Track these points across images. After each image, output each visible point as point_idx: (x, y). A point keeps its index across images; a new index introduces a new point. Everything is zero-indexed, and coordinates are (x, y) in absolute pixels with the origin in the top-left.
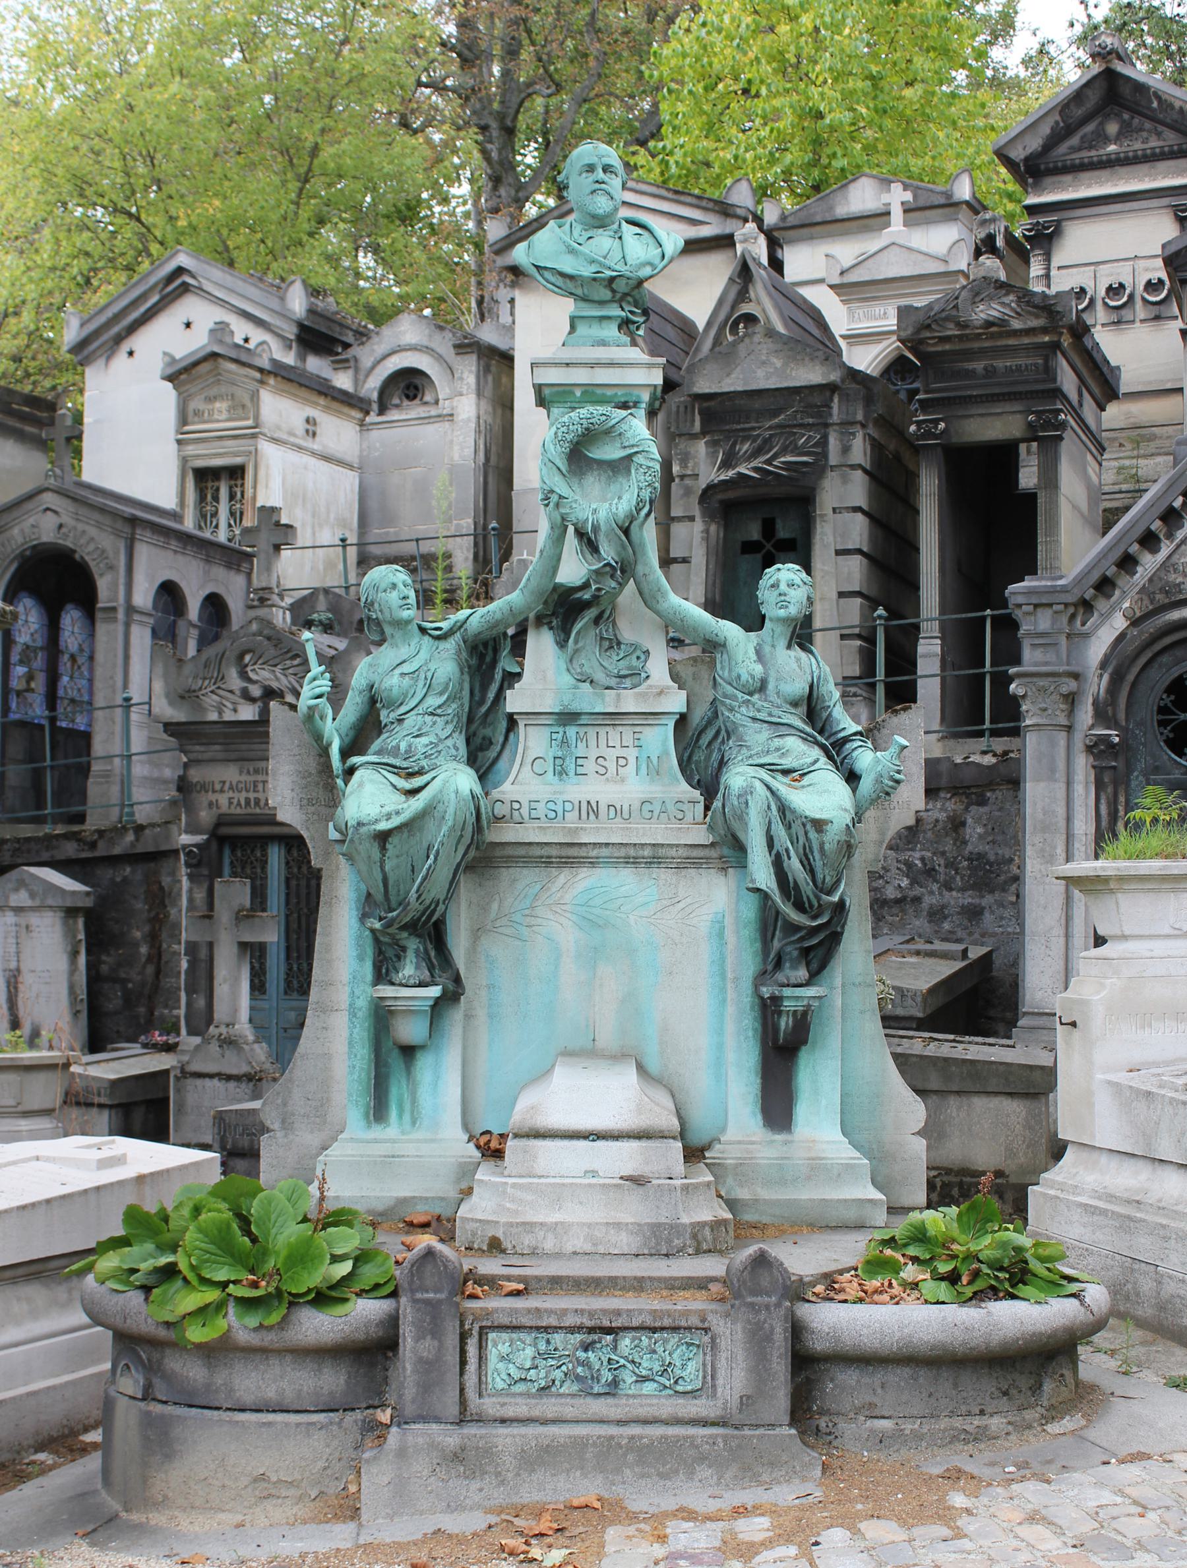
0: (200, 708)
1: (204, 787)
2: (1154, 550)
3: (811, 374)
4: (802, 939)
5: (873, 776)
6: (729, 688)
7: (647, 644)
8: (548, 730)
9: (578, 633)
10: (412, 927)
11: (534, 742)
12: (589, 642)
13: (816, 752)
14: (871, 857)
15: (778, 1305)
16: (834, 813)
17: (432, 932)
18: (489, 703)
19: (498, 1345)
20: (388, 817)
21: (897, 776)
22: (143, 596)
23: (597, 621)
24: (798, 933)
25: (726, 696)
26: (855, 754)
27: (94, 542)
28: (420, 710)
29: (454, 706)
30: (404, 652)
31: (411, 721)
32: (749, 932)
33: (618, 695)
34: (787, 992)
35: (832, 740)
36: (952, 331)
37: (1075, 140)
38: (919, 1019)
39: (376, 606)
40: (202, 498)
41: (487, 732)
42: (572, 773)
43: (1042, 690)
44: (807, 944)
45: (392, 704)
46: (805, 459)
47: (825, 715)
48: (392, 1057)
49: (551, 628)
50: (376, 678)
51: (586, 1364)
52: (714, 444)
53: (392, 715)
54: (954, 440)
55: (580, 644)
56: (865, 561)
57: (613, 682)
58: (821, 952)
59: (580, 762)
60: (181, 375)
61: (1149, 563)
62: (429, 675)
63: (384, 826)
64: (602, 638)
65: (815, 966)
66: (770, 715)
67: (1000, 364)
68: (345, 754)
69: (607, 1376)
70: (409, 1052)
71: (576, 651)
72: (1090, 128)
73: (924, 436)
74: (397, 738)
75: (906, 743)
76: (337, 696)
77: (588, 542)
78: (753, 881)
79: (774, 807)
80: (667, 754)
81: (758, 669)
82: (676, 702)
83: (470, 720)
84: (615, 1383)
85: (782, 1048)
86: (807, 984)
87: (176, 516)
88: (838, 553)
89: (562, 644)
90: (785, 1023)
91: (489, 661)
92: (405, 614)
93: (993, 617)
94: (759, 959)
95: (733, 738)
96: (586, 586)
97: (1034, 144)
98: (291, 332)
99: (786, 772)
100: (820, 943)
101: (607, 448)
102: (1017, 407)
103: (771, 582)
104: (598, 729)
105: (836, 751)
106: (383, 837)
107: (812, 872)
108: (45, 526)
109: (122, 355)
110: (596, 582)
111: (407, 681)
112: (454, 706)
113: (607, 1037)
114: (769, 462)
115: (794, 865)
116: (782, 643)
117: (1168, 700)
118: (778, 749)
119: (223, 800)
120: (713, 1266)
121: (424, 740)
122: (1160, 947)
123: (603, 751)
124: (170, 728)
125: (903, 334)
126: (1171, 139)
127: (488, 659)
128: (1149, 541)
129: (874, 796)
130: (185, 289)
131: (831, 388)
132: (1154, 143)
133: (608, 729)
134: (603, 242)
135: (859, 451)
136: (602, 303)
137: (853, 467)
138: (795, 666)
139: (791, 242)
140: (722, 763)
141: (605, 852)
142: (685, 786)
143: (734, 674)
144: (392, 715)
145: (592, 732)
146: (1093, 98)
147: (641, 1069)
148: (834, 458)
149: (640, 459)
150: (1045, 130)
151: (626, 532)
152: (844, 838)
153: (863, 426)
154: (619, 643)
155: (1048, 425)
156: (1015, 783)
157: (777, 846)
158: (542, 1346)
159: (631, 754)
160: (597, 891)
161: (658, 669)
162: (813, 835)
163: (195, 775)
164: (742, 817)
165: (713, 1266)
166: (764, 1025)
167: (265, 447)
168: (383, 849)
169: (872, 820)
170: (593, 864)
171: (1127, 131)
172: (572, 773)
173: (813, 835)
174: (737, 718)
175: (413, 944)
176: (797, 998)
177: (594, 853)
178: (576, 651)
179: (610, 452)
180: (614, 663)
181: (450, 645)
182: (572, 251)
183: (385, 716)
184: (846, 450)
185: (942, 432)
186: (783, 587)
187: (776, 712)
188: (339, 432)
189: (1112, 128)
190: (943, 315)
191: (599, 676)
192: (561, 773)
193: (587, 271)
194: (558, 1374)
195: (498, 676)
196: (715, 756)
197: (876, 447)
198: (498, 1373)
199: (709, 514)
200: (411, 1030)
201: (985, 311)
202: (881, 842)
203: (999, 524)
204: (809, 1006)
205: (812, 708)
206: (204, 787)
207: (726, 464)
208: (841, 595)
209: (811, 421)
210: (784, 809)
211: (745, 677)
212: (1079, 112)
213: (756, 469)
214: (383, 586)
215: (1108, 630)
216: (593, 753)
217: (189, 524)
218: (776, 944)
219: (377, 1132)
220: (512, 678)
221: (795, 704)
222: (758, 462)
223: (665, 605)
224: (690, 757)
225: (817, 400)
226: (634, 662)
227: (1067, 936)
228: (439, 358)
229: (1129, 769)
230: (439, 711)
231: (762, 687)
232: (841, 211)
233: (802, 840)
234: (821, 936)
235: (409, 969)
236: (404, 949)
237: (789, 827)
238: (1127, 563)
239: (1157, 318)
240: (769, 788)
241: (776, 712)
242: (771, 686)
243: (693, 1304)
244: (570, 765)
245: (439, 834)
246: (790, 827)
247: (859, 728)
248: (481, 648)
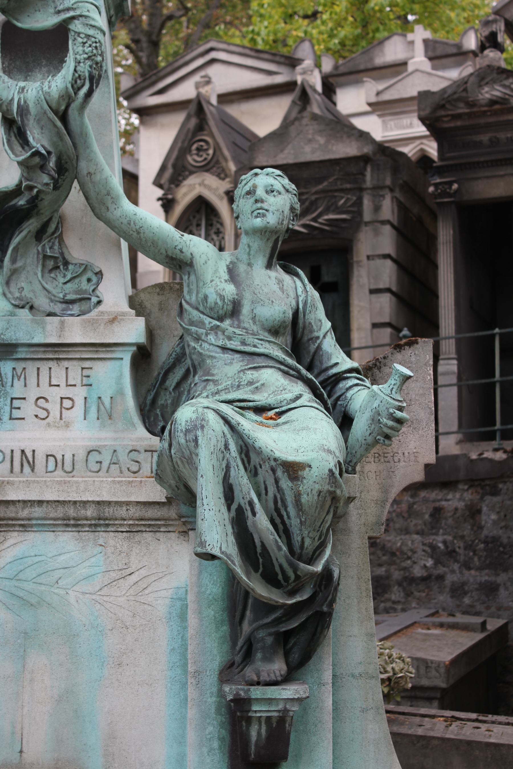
3: (348, 149)
4: (277, 621)
5: (367, 415)
6: (195, 313)
7: (100, 264)
9: (16, 249)
12: (31, 260)
13: (299, 388)
14: (372, 519)
16: (314, 455)
21: (399, 414)
23: (39, 235)
25: (192, 323)
26: (349, 394)
32: (214, 612)
33: (62, 323)
34: (256, 692)
35: (322, 378)
36: (462, 109)
38: (443, 690)
42: (6, 417)
44: (284, 628)
46: (344, 216)
47: (313, 348)
55: (19, 264)
56: (394, 299)
57: (58, 308)
59: (16, 403)
64: (46, 257)
65: (295, 656)
66: (243, 343)
67: (502, 136)
71: (14, 272)
73: (440, 196)
75: (409, 373)
78: (202, 544)
79: (233, 447)
80: (121, 392)
81: (230, 290)
82: (133, 331)
86: (287, 679)
88: (372, 292)
90: (255, 733)
93: (501, 335)
94: (226, 647)
95: (200, 373)
99: (260, 410)
100: (302, 627)
101: (39, 15)
103: (247, 188)
104: (38, 364)
105: (327, 390)
110: (27, 179)
114: (315, 220)
116: (260, 262)
118: (250, 383)
123: (45, 390)
125: (423, 114)
129: (370, 439)
131: (364, 160)
133: (51, 364)
135: (388, 209)
137: (383, 222)
138: (276, 288)
139: (342, 85)
141: (38, 512)
143: (201, 296)
145: (31, 368)
151: (64, 117)
152: (327, 487)
153: (391, 190)
154: (66, 263)
157: (239, 499)
159: (79, 394)
160: (29, 561)
161: (114, 293)
162: (285, 484)
164: (191, 460)
169: (372, 475)
170: (25, 528)
172: (6, 417)
173: (285, 484)
174: (204, 348)
176: (270, 701)
177: (25, 513)
178: (14, 272)
180: (59, 286)
184: (377, 209)
185: (456, 191)
186: (260, 192)
187: (250, 339)
190: (455, 96)
191: (42, 302)
197: (402, 208)
202: (384, 502)
204: (285, 711)
208: (375, 326)
209: (348, 186)
211: (213, 298)
213: (304, 226)
216: (32, 393)
218: (246, 628)
221: (275, 331)
222: (306, 220)
223: (118, 213)
224: (154, 401)
226: (85, 286)
231: (234, 310)
232: (379, 61)
233: (272, 490)
234: (302, 618)
237: (253, 473)
240: (226, 421)
241: (250, 339)
242: (245, 310)
246: (256, 474)
247: (355, 365)
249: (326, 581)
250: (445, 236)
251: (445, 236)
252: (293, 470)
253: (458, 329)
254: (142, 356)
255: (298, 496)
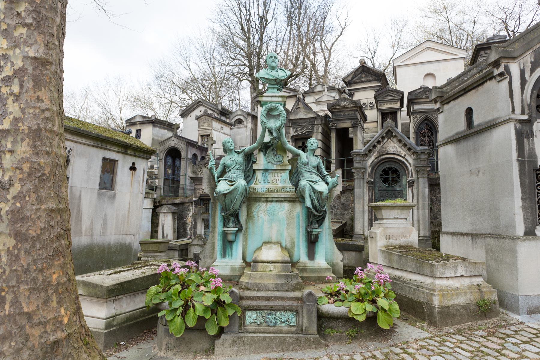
0: (197, 174)
1: (198, 189)
2: (380, 144)
3: (311, 115)
8: (261, 173)
10: (231, 215)
11: (259, 175)
13: (319, 178)
15: (314, 305)
17: (236, 216)
19: (248, 314)
20: (226, 190)
22: (190, 156)
24: (314, 217)
27: (181, 146)
30: (231, 156)
31: (232, 171)
34: (314, 230)
37: (357, 78)
40: (202, 140)
41: (249, 174)
43: (358, 171)
45: (229, 167)
48: (228, 243)
49: (262, 151)
51: (269, 318)
52: (293, 128)
54: (338, 127)
58: (321, 221)
60: (198, 118)
61: (379, 147)
63: (225, 192)
67: (346, 113)
68: (218, 178)
69: (274, 321)
70: (231, 242)
72: (359, 76)
74: (229, 175)
76: (217, 165)
77: (271, 133)
82: (290, 167)
83: (245, 171)
84: (276, 323)
85: (312, 241)
86: (318, 228)
87: (197, 143)
89: (265, 155)
91: (249, 157)
92: (231, 148)
96: (270, 142)
97: (349, 78)
98: (218, 112)
99: (313, 182)
102: (350, 121)
105: (323, 178)
106: (225, 195)
107: (319, 203)
108: (173, 143)
109: (189, 116)
113: (274, 239)
115: (316, 202)
116: (312, 155)
117: (382, 173)
119: (201, 192)
120: (297, 294)
121: (235, 175)
122: (390, 221)
124: (191, 178)
126: (374, 78)
128: (379, 142)
130: (200, 105)
131: (315, 118)
132: (371, 78)
134: (274, 73)
136: (274, 85)
140: (299, 180)
142: (291, 185)
146: (360, 70)
147: (282, 247)
148: (315, 131)
149: (282, 115)
150: (351, 76)
155: (355, 124)
156: (352, 190)
158: (258, 314)
159: (279, 178)
163: (196, 187)
165: (297, 294)
166: (308, 237)
167: (213, 131)
168: (225, 198)
171: (366, 76)
174: (302, 171)
175: (232, 219)
179: (276, 113)
181: (241, 155)
182: (268, 74)
183: (227, 170)
184: (318, 129)
188: (227, 129)
189: (364, 76)
191: (273, 162)
192: (265, 182)
193: (271, 78)
194: (262, 321)
195: (251, 162)
196: (297, 179)
197: (323, 129)
198: (248, 320)
199: (293, 141)
200: (231, 238)
201: (343, 104)
203: (346, 142)
205: (318, 168)
206: (198, 189)
207: (296, 131)
210: (313, 189)
212: (357, 73)
215: (371, 160)
216: (271, 178)
217: (200, 144)
218: (311, 219)
219: (224, 260)
220: (254, 162)
221: (315, 168)
222: (302, 131)
225: (312, 120)
227: (363, 219)
228: (244, 117)
229: (375, 187)
235: (231, 225)
236: (230, 220)
238: (375, 146)
239: (372, 109)
243: (295, 304)
244: (266, 180)
245: (238, 194)
249: (325, 211)
250: (333, 135)
251: (333, 135)
252: (321, 193)
253: (336, 158)
254: (290, 171)
255: (321, 197)
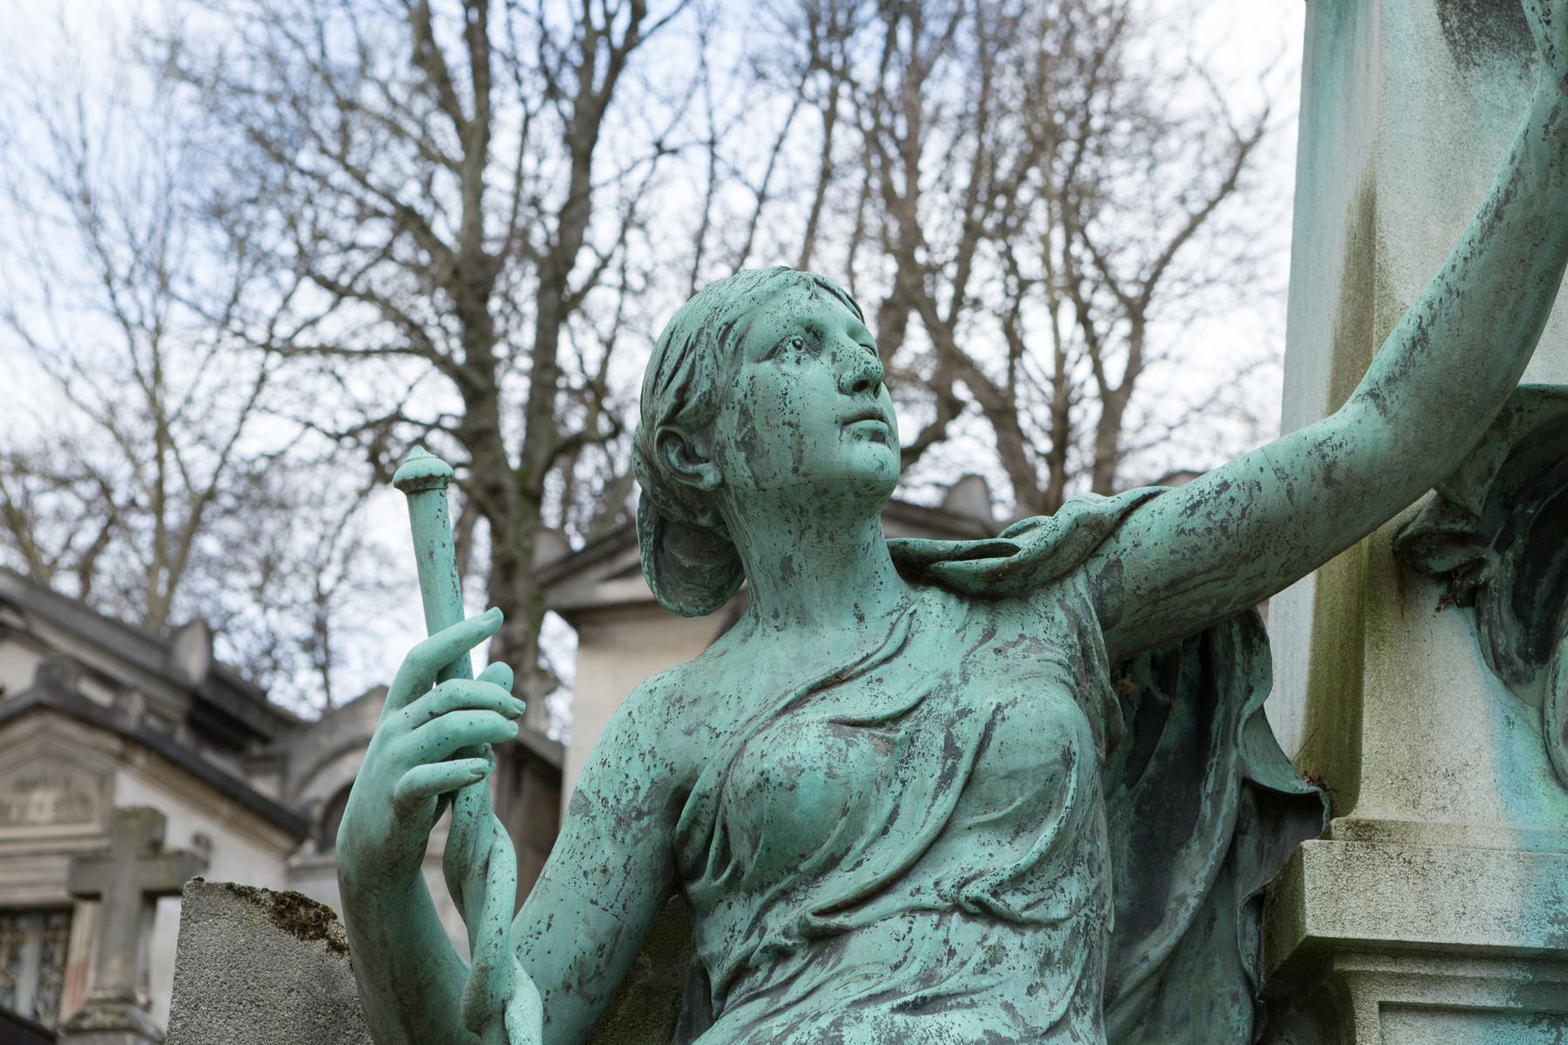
18: (1179, 920)
28: (926, 886)
29: (1074, 888)
30: (836, 643)
31: (875, 942)
39: (727, 426)
49: (1465, 593)
50: (709, 759)
53: (780, 921)
62: (969, 733)
111: (863, 752)
112: (1074, 888)
127: (1171, 735)
144: (780, 921)
181: (1047, 631)
183: (725, 937)
195: (1220, 809)
214: (765, 328)
230: (1015, 902)
248: (1147, 678)
